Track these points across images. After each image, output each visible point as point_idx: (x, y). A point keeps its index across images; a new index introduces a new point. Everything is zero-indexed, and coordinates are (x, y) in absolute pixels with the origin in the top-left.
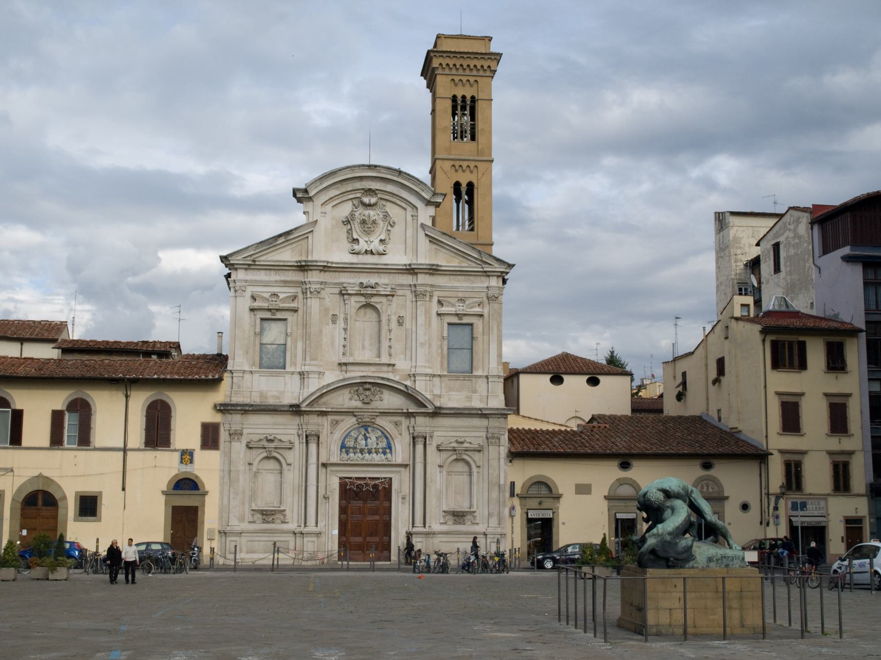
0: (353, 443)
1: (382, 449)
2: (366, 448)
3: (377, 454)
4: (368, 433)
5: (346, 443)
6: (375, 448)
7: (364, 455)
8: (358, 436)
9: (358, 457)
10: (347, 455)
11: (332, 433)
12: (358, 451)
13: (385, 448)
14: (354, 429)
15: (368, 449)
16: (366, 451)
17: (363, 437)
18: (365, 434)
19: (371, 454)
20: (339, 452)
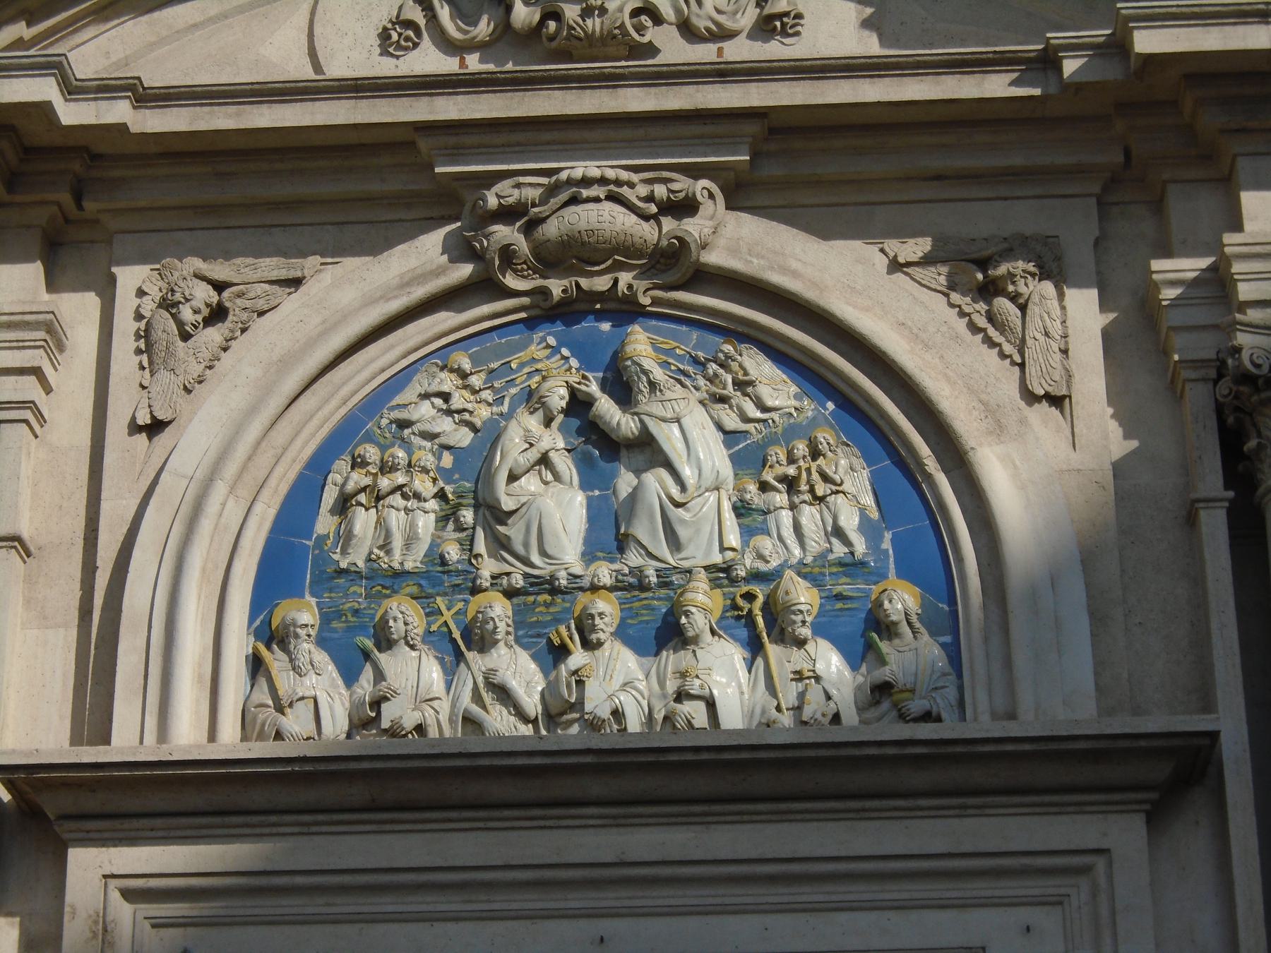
0: (426, 523)
1: (803, 571)
2: (605, 573)
3: (755, 647)
4: (622, 389)
5: (325, 523)
6: (722, 574)
7: (578, 658)
8: (490, 437)
9: (503, 694)
10: (350, 677)
11: (155, 427)
12: (500, 610)
13: (851, 566)
14: (440, 356)
15: (630, 586)
16: (606, 609)
17: (553, 440)
18: (579, 404)
19: (671, 660)
20: (238, 644)
